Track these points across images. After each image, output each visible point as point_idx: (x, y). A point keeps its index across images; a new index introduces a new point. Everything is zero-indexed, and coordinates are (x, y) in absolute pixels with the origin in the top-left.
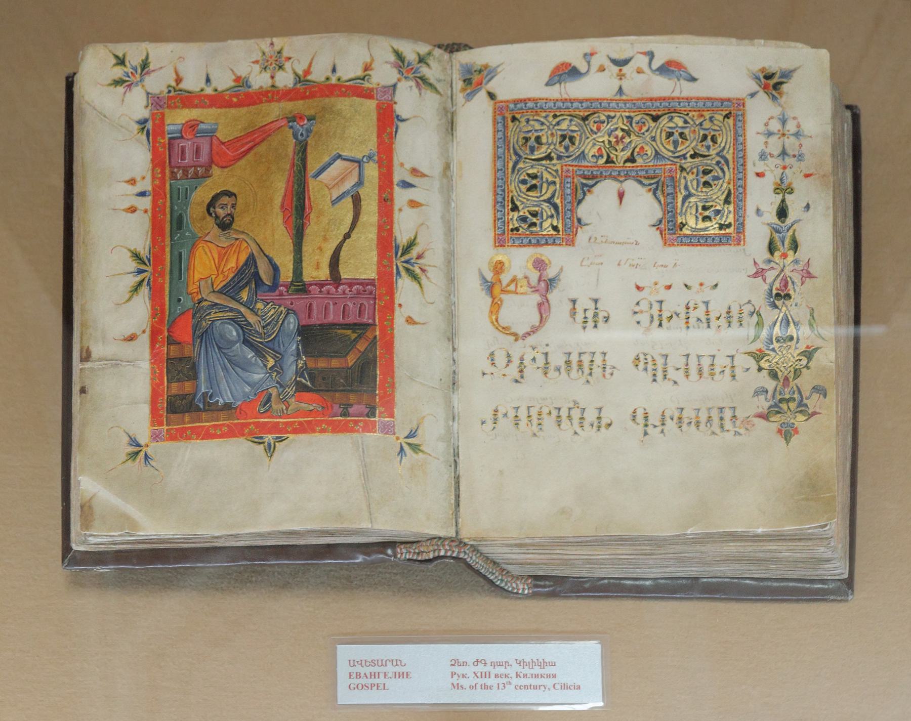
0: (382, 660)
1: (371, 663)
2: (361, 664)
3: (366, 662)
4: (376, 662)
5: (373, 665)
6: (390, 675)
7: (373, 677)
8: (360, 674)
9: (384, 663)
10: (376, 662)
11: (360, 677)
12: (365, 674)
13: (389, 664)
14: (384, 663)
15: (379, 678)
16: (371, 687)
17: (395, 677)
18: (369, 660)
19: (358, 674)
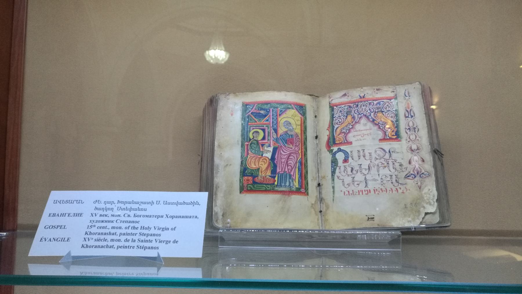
0: (72, 200)
1: (66, 202)
2: (60, 202)
3: (63, 201)
4: (68, 202)
5: (67, 202)
6: (71, 215)
7: (62, 216)
8: (55, 214)
9: (72, 202)
10: (68, 202)
11: (55, 216)
12: (58, 214)
13: (75, 202)
14: (72, 202)
15: (65, 216)
16: (57, 227)
17: (74, 216)
18: (65, 200)
19: (54, 214)
